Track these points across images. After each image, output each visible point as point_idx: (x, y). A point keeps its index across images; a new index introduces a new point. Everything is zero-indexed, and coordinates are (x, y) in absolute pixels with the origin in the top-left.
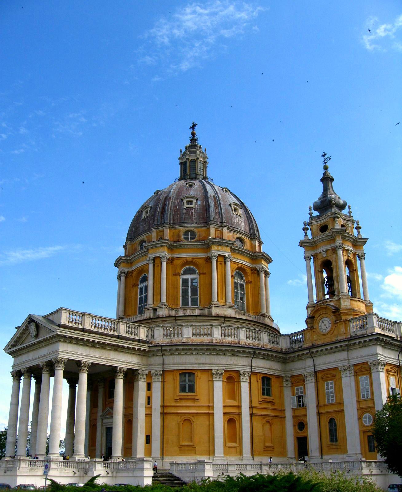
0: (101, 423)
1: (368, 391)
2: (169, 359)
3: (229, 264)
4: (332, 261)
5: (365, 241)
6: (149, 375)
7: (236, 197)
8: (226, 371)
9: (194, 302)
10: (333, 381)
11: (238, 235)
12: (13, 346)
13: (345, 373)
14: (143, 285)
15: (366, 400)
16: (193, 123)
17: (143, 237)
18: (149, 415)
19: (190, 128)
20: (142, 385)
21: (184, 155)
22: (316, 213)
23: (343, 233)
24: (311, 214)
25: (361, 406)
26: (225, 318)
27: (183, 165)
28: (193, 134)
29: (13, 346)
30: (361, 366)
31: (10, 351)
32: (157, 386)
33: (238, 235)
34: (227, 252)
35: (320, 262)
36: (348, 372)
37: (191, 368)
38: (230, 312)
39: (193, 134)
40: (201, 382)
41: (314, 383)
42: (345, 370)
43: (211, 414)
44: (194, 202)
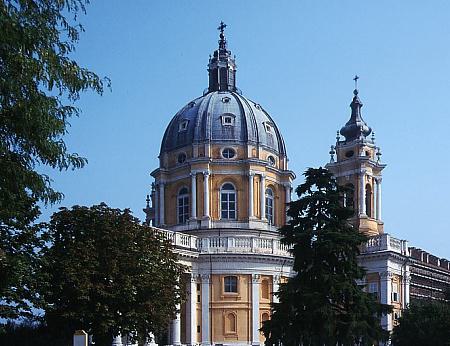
2: (215, 265)
3: (264, 181)
5: (383, 167)
6: (199, 278)
7: (269, 117)
8: (263, 276)
9: (232, 215)
11: (270, 154)
14: (186, 195)
17: (183, 151)
18: (200, 310)
20: (194, 286)
21: (214, 61)
22: (343, 138)
23: (366, 160)
24: (338, 138)
26: (260, 231)
27: (213, 73)
28: (222, 36)
32: (206, 287)
33: (270, 154)
34: (262, 171)
38: (266, 228)
39: (222, 36)
40: (243, 286)
43: (249, 310)
44: (232, 120)
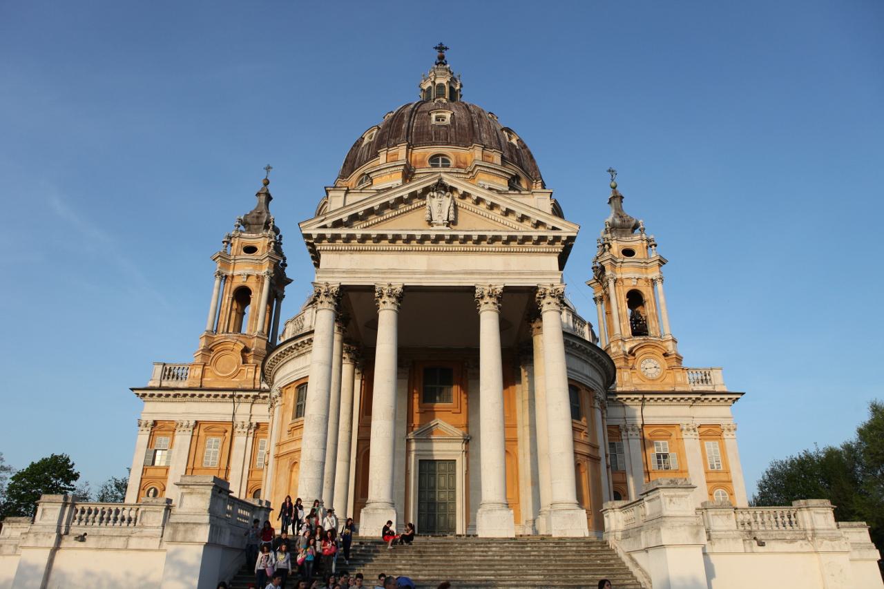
0: (405, 449)
1: (719, 461)
4: (645, 293)
10: (667, 442)
12: (338, 224)
13: (688, 433)
15: (717, 472)
16: (441, 44)
19: (436, 48)
25: (710, 479)
29: (338, 224)
30: (707, 429)
31: (328, 232)
35: (627, 290)
36: (692, 432)
37: (580, 380)
39: (441, 58)
41: (639, 440)
42: (688, 430)
